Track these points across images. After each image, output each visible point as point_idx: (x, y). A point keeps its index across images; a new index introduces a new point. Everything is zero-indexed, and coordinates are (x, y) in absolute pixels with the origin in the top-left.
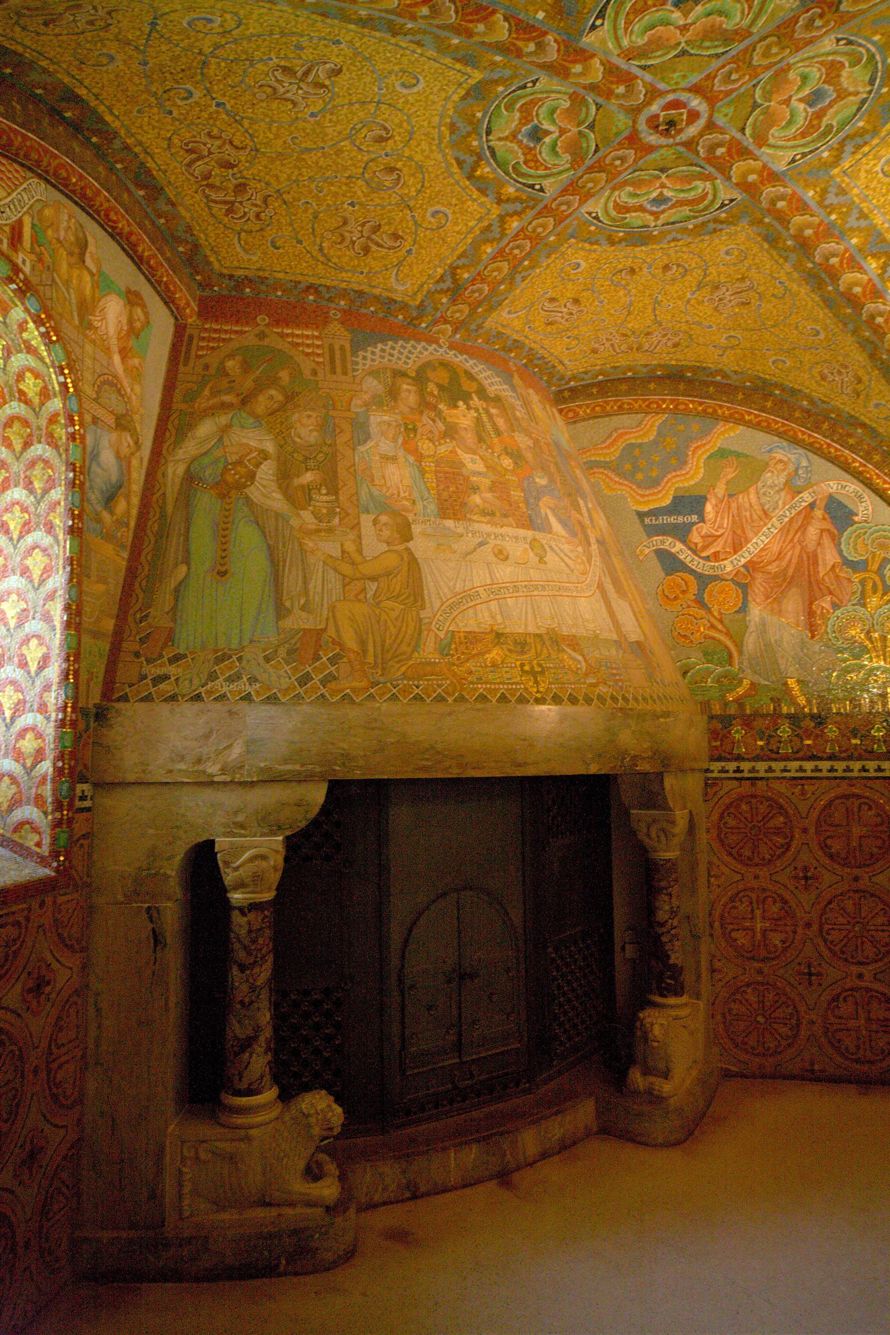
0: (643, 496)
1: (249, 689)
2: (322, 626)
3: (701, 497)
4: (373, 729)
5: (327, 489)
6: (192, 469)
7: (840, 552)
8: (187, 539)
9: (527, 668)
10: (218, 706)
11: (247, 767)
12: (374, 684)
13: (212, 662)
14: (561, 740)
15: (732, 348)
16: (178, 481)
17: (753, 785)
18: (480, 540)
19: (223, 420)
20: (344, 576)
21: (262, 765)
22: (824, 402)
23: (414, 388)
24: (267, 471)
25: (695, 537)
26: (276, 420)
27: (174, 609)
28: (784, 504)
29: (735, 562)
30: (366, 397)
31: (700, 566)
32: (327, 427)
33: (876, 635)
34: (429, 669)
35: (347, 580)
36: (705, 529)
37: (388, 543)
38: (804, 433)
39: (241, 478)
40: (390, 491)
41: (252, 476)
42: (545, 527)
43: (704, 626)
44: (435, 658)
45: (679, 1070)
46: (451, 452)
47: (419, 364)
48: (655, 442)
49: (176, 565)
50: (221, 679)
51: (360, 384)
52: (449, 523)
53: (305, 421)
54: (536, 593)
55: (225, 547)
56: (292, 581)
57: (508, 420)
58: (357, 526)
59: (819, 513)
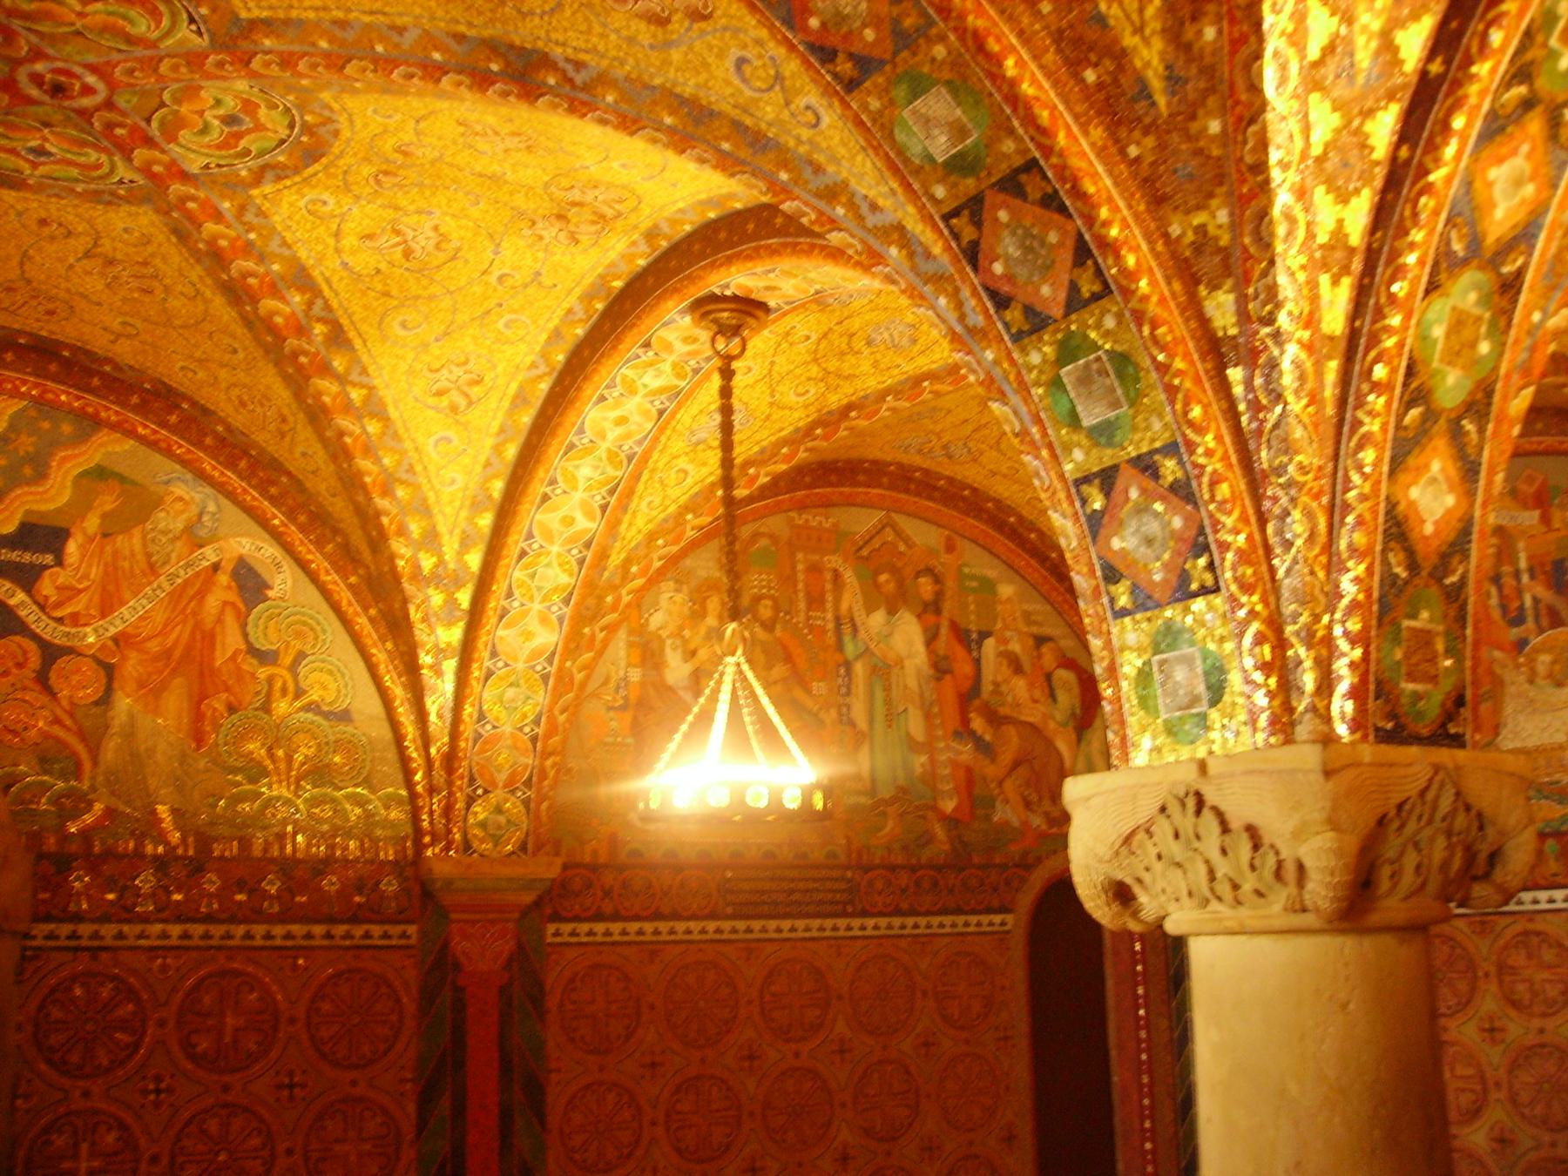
7: (245, 635)
15: (129, 336)
17: (94, 958)
25: (46, 587)
29: (101, 631)
33: (280, 753)
36: (63, 576)
43: (46, 718)
59: (223, 578)
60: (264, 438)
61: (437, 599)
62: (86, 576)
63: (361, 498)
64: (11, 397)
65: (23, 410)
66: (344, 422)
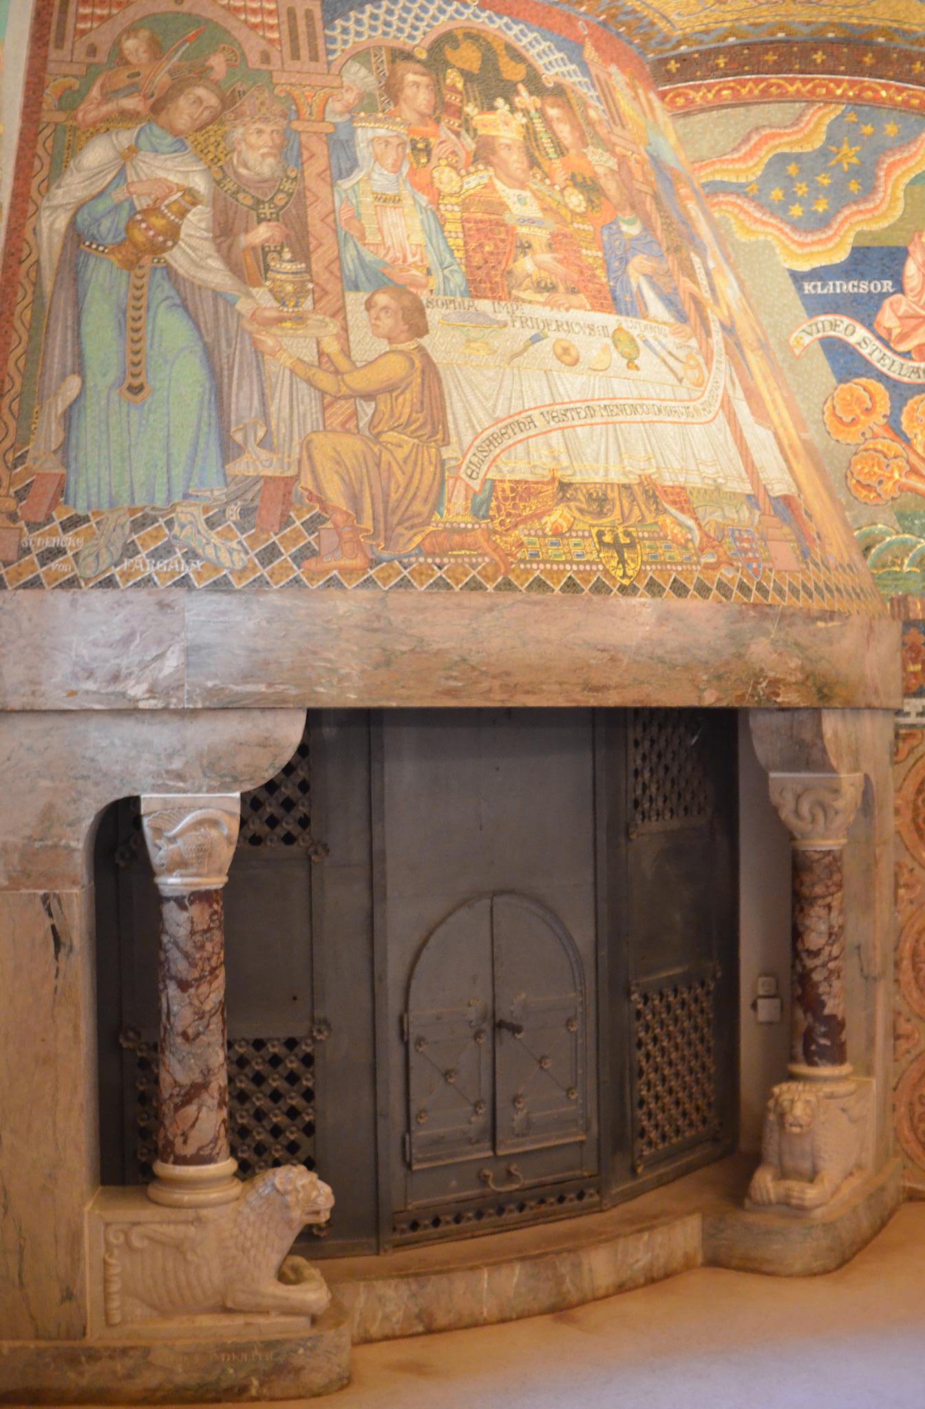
0: (802, 245)
1: (185, 569)
2: (291, 473)
3: (898, 249)
4: (375, 630)
5: (293, 252)
6: (79, 219)
8: (78, 336)
9: (608, 538)
10: (142, 595)
11: (187, 687)
12: (374, 562)
13: (127, 530)
14: (659, 652)
16: (58, 241)
18: (534, 332)
19: (125, 138)
20: (323, 394)
21: (210, 684)
23: (424, 80)
24: (197, 224)
25: (888, 318)
26: (207, 140)
27: (65, 447)
30: (350, 97)
31: (896, 367)
32: (289, 149)
34: (457, 538)
35: (328, 399)
36: (904, 304)
37: (391, 340)
39: (157, 235)
40: (391, 254)
41: (173, 233)
42: (636, 309)
43: (900, 469)
44: (466, 521)
45: (832, 1170)
46: (486, 186)
47: (432, 36)
48: (823, 153)
49: (63, 377)
50: (144, 554)
51: (340, 75)
52: (484, 305)
53: (253, 139)
54: (621, 418)
55: (137, 347)
56: (243, 402)
57: (576, 127)
58: (339, 312)
64: (827, 103)
65: (843, 115)
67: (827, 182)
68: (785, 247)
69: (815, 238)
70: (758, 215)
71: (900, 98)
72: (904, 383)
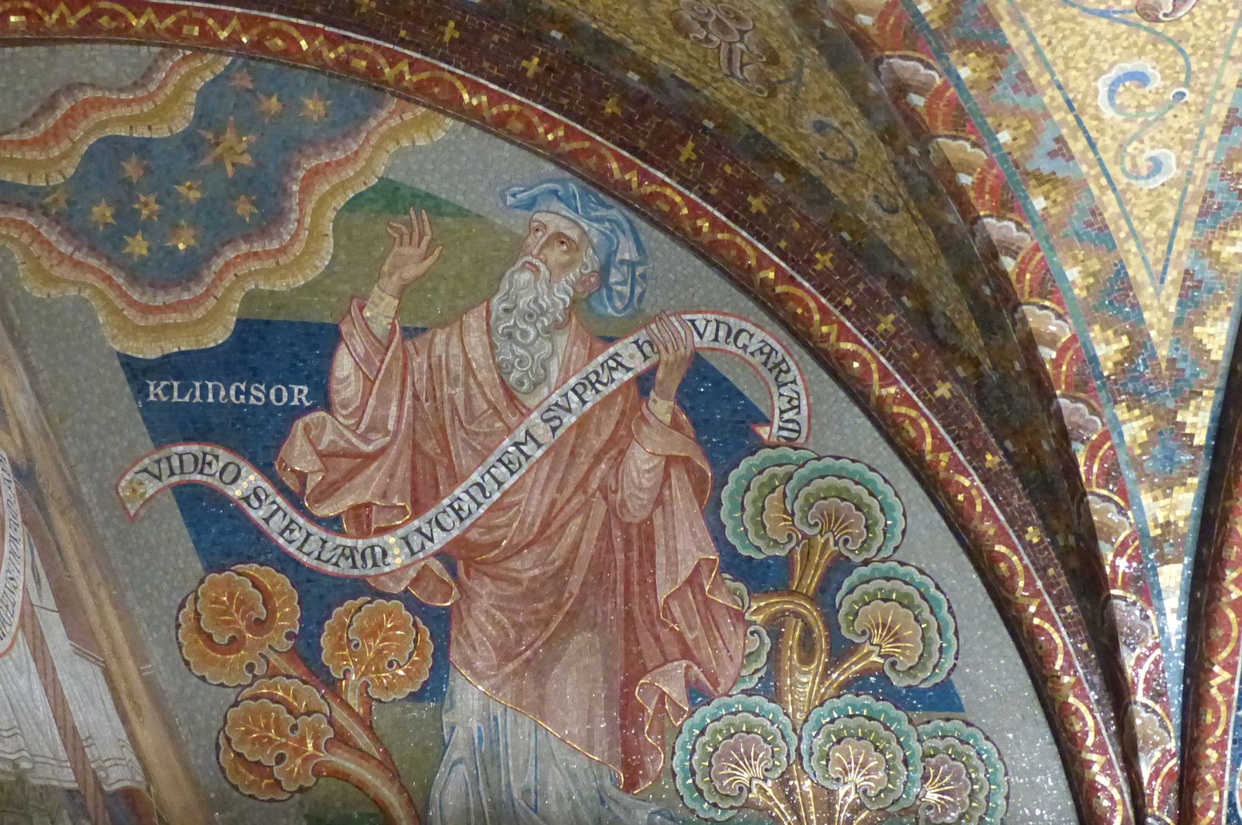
0: (145, 310)
3: (322, 326)
22: (683, 85)
25: (299, 455)
28: (566, 374)
29: (416, 541)
31: (313, 545)
36: (331, 430)
38: (626, 166)
48: (190, 142)
59: (661, 407)
60: (731, 92)
61: (1135, 429)
62: (377, 426)
63: (952, 217)
64: (199, 51)
65: (226, 75)
66: (908, 67)
67: (194, 195)
68: (117, 312)
69: (171, 299)
70: (66, 249)
71: (332, 55)
72: (326, 575)
